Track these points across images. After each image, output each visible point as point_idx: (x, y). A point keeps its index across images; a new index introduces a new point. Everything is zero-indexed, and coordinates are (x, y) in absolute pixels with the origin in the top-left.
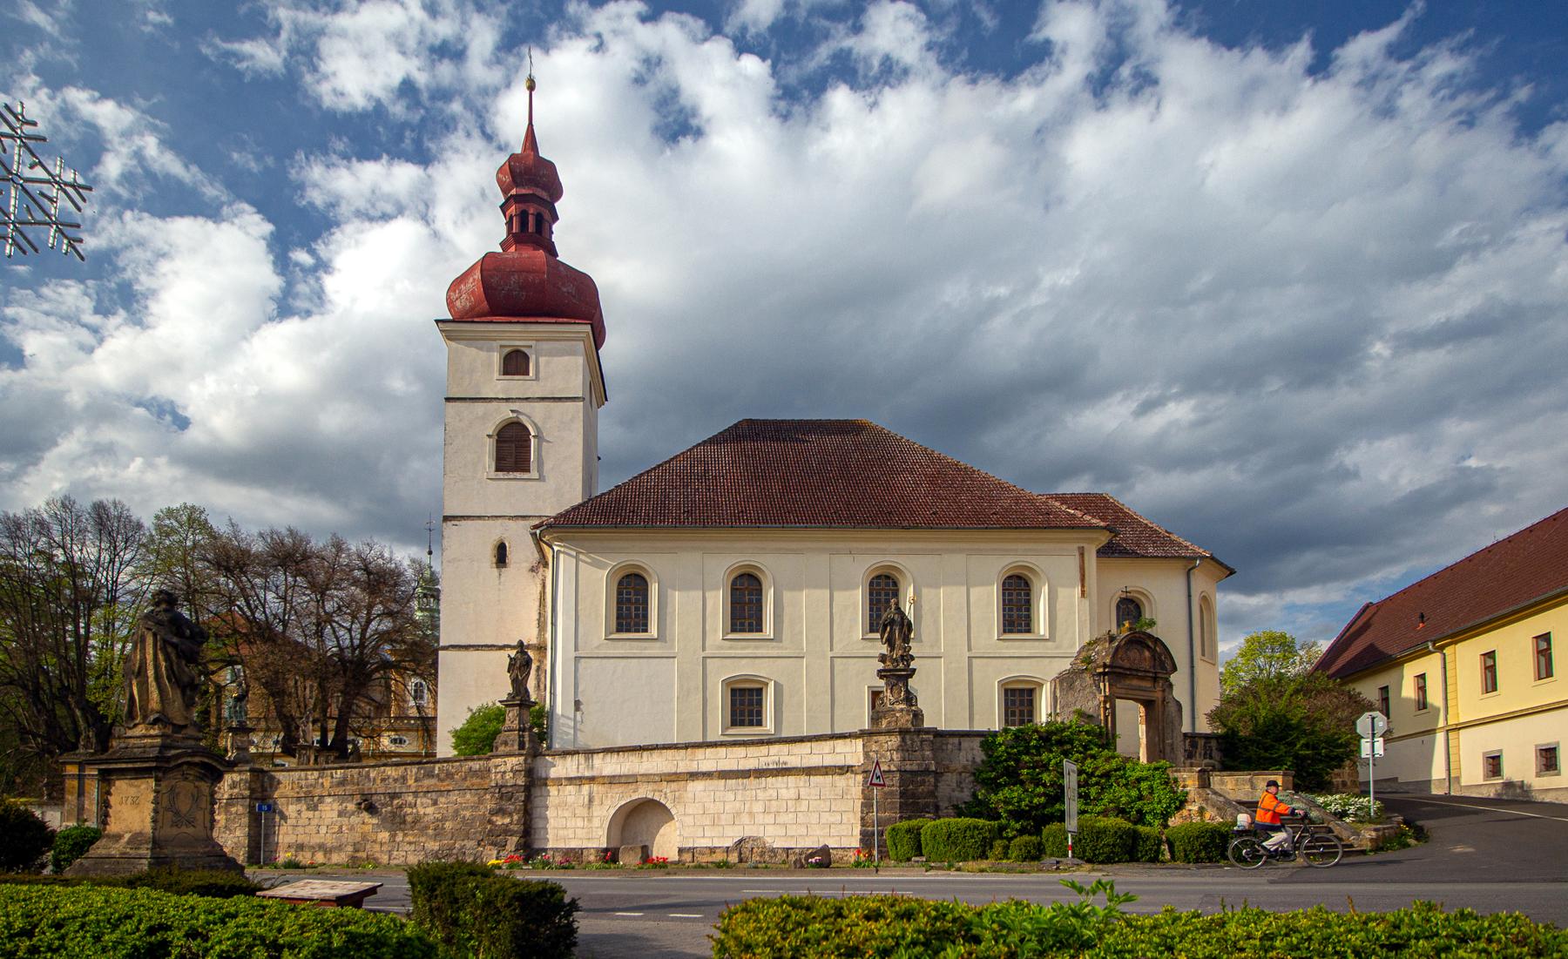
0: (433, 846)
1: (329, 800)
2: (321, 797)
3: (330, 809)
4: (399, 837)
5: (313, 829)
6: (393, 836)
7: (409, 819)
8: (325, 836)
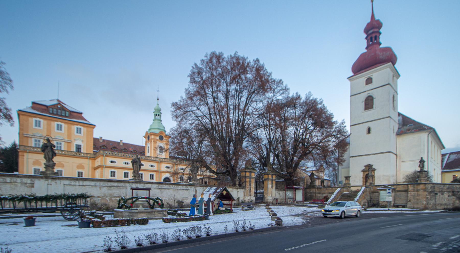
3: (446, 195)
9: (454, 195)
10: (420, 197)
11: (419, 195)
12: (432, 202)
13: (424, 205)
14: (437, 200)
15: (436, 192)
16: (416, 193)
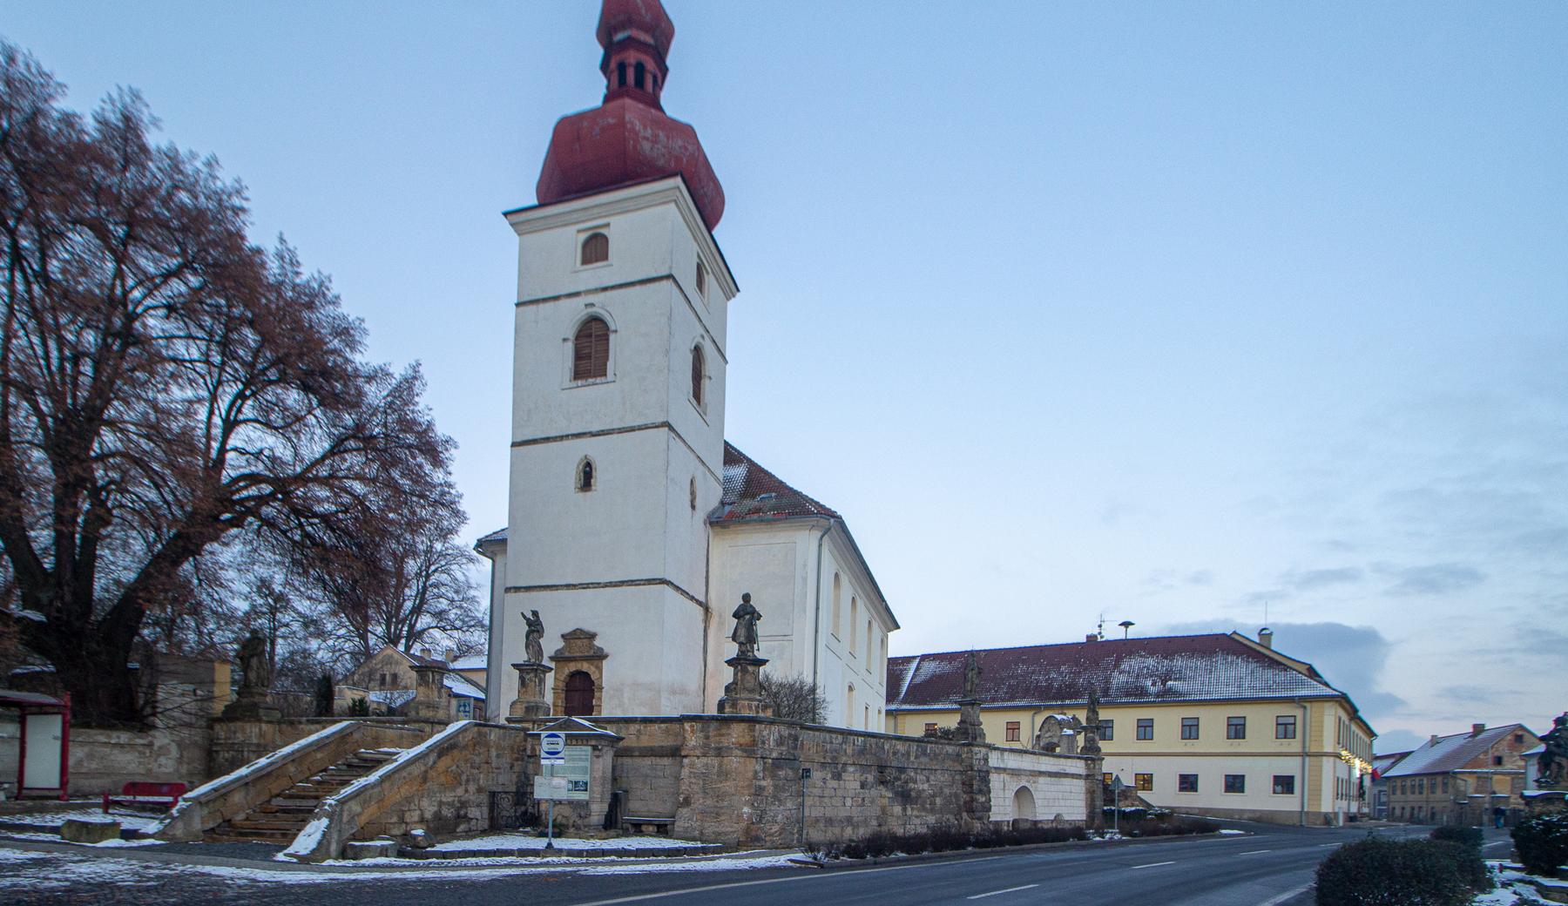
0: (931, 819)
1: (851, 769)
2: (845, 764)
3: (852, 779)
4: (909, 812)
5: (837, 802)
6: (905, 810)
7: (913, 794)
8: (848, 808)
9: (882, 783)
10: (728, 786)
11: (724, 774)
12: (781, 812)
13: (744, 825)
14: (809, 802)
15: (807, 765)
16: (716, 761)
